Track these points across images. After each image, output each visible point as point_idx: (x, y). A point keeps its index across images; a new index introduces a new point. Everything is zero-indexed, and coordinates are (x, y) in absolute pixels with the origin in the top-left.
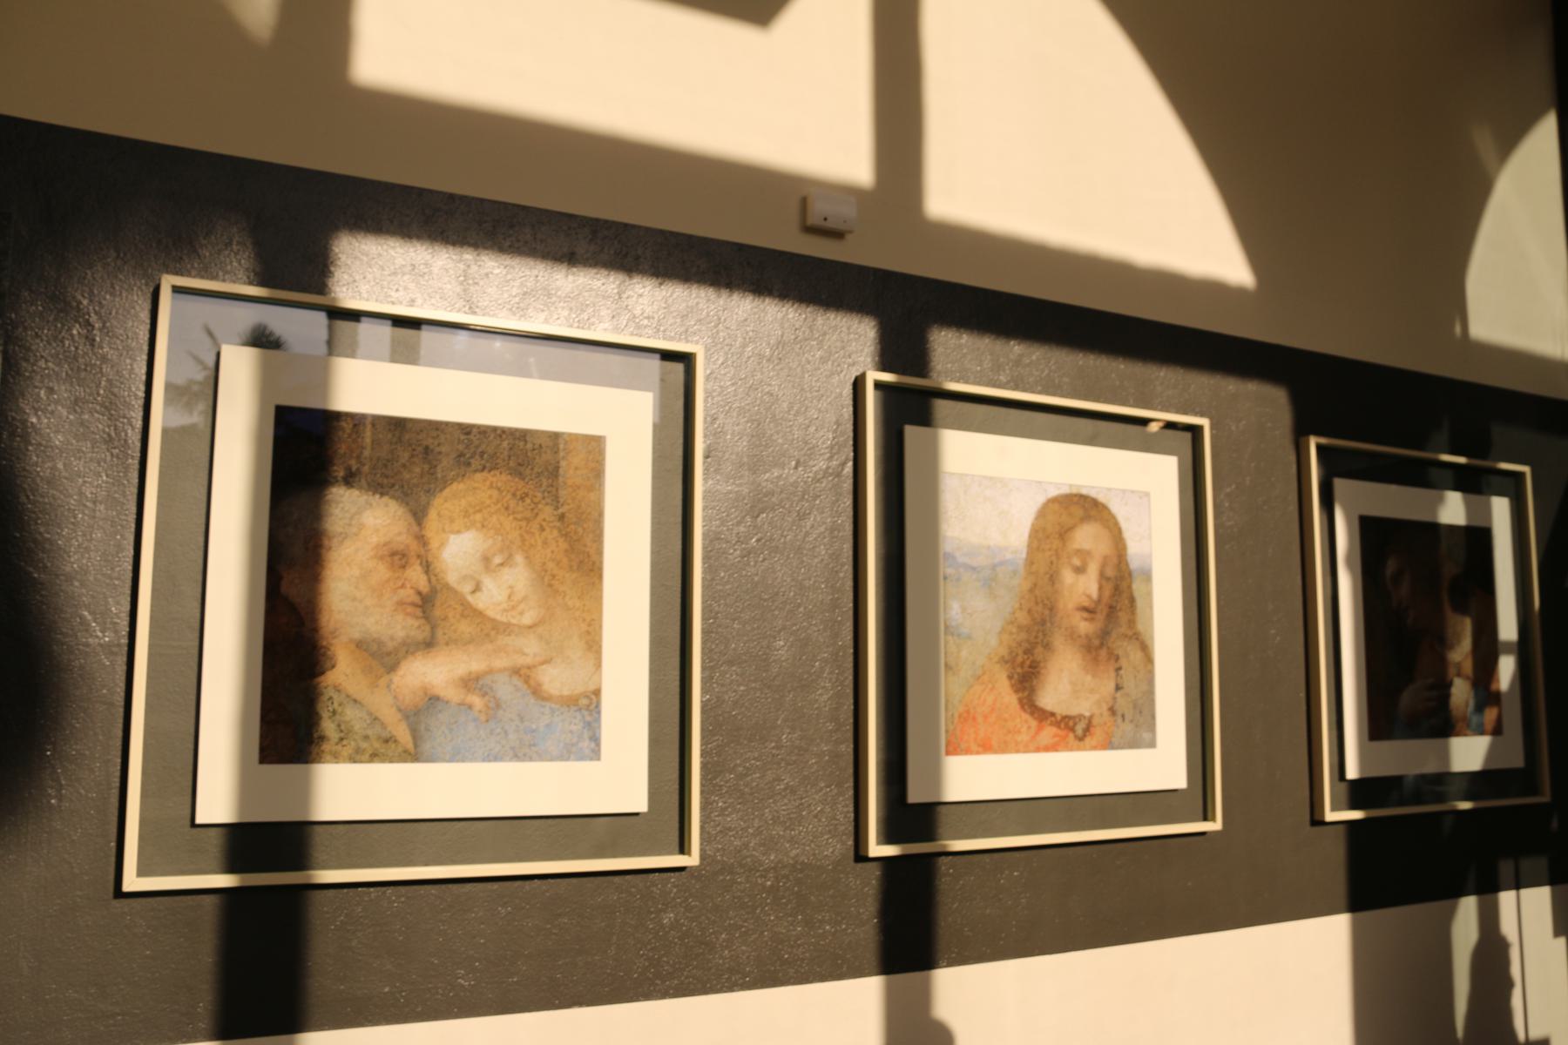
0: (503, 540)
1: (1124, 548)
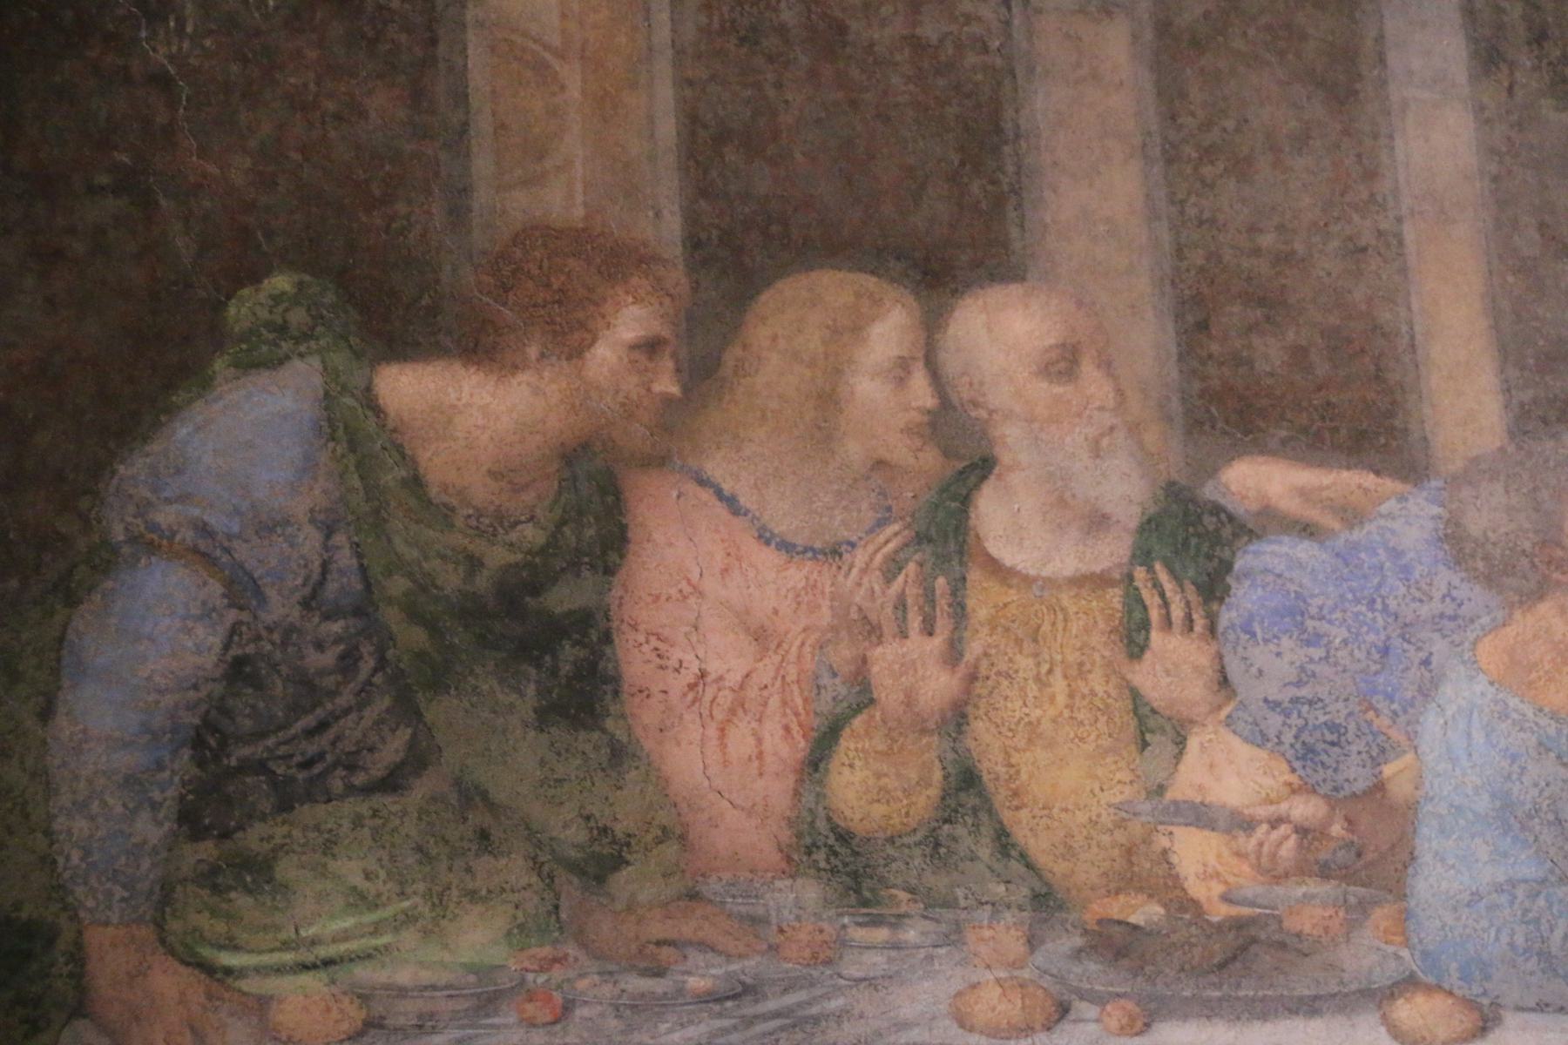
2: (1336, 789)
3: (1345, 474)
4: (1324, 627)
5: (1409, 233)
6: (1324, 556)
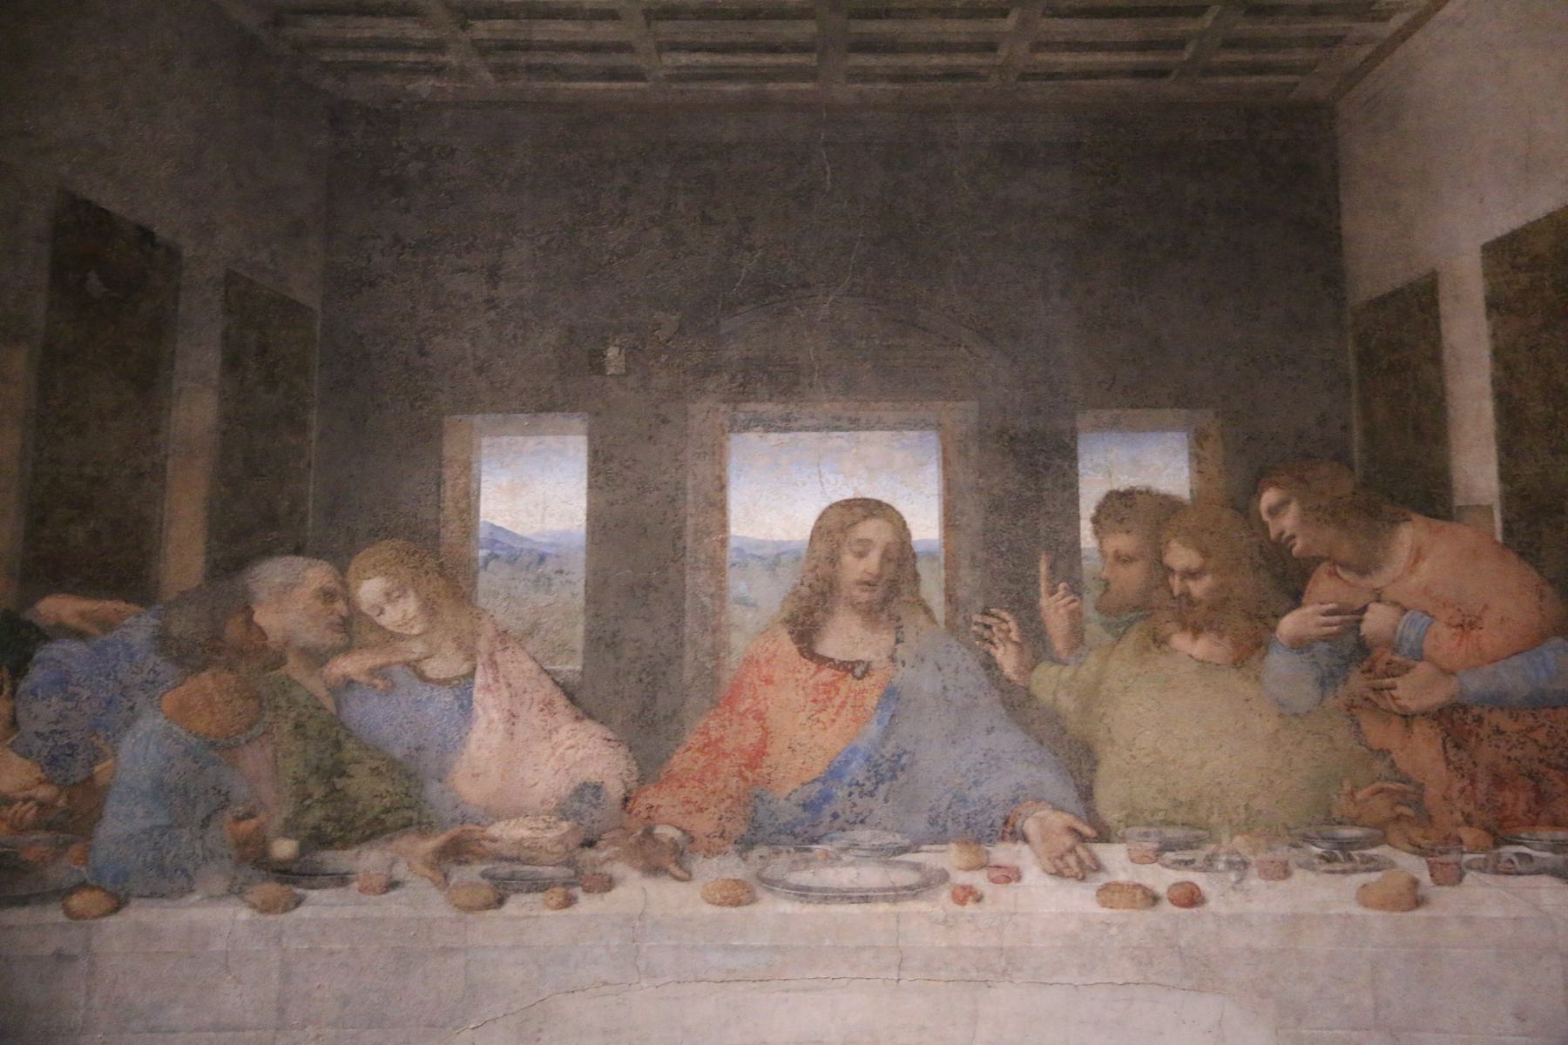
1: (909, 535)
2: (65, 780)
3: (108, 603)
4: (77, 690)
5: (170, 463)
6: (87, 650)
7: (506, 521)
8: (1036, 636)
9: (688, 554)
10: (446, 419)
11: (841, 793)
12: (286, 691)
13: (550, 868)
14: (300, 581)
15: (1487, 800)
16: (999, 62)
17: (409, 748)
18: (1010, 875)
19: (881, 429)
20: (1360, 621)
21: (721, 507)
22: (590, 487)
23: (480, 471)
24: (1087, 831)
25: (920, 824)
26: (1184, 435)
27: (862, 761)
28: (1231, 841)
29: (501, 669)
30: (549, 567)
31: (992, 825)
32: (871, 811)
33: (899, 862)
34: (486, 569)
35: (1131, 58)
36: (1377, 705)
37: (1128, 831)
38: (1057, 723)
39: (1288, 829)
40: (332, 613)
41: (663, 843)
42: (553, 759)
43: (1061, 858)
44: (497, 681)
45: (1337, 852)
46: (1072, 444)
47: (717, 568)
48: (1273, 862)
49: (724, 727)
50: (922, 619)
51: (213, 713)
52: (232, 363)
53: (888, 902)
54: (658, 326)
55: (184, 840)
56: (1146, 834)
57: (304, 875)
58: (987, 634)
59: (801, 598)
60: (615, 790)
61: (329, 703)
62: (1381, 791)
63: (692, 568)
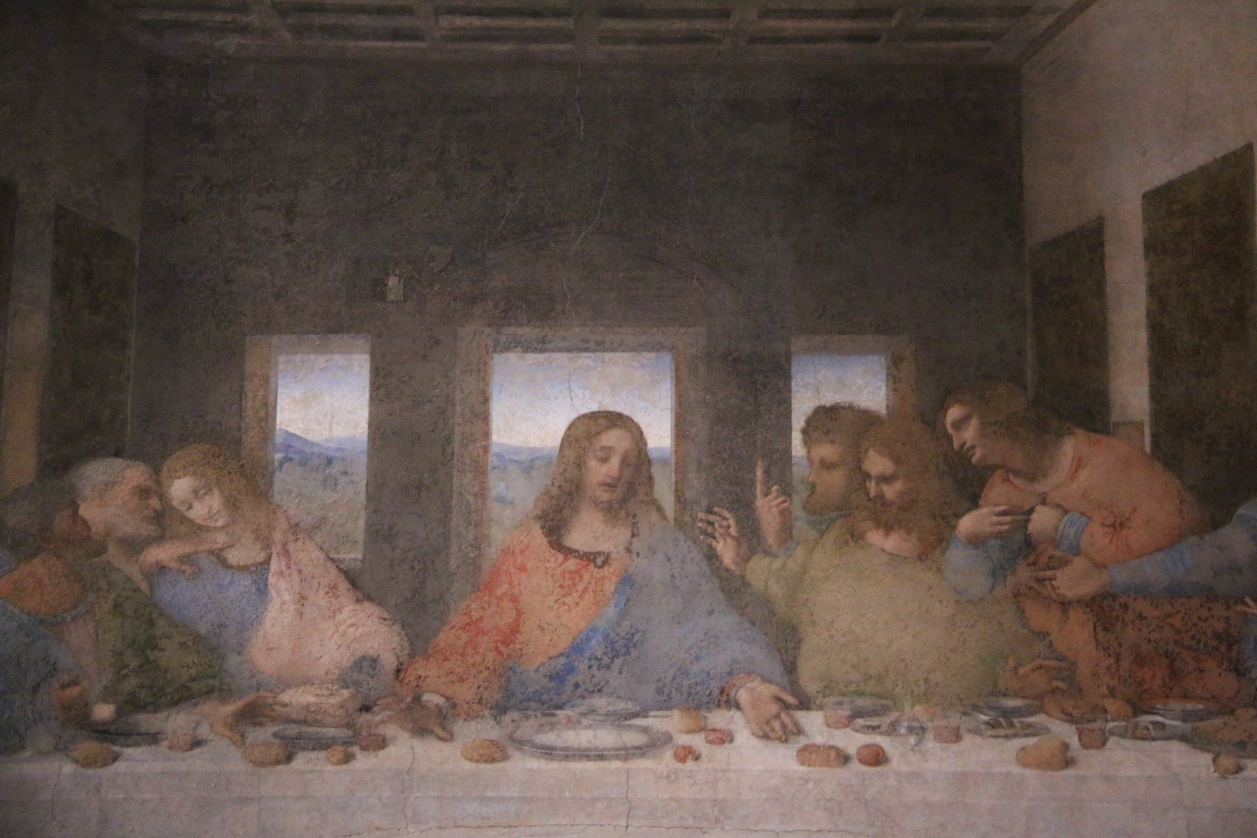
0: (206, 480)
1: (645, 444)
7: (299, 428)
8: (752, 532)
9: (455, 458)
10: (248, 338)
11: (582, 666)
12: (106, 576)
13: (333, 729)
14: (120, 480)
15: (1130, 677)
16: (731, 26)
17: (212, 625)
18: (724, 738)
19: (624, 351)
20: (1027, 521)
21: (485, 418)
22: (372, 399)
23: (277, 385)
24: (791, 700)
25: (648, 692)
26: (883, 359)
27: (601, 639)
28: (912, 710)
29: (293, 557)
30: (336, 468)
31: (710, 694)
32: (607, 682)
33: (630, 726)
34: (281, 470)
35: (846, 25)
36: (1039, 594)
37: (826, 700)
38: (767, 607)
39: (961, 700)
40: (146, 508)
41: (429, 708)
42: (335, 636)
43: (768, 723)
44: (289, 568)
45: (1001, 719)
46: (786, 365)
47: (480, 470)
48: (946, 728)
49: (484, 608)
50: (654, 516)
51: (42, 594)
52: (62, 288)
53: (620, 759)
54: (432, 259)
55: (17, 704)
56: (841, 703)
57: (120, 735)
58: (710, 529)
59: (552, 498)
60: (389, 662)
61: (144, 586)
62: (1041, 667)
63: (458, 470)
